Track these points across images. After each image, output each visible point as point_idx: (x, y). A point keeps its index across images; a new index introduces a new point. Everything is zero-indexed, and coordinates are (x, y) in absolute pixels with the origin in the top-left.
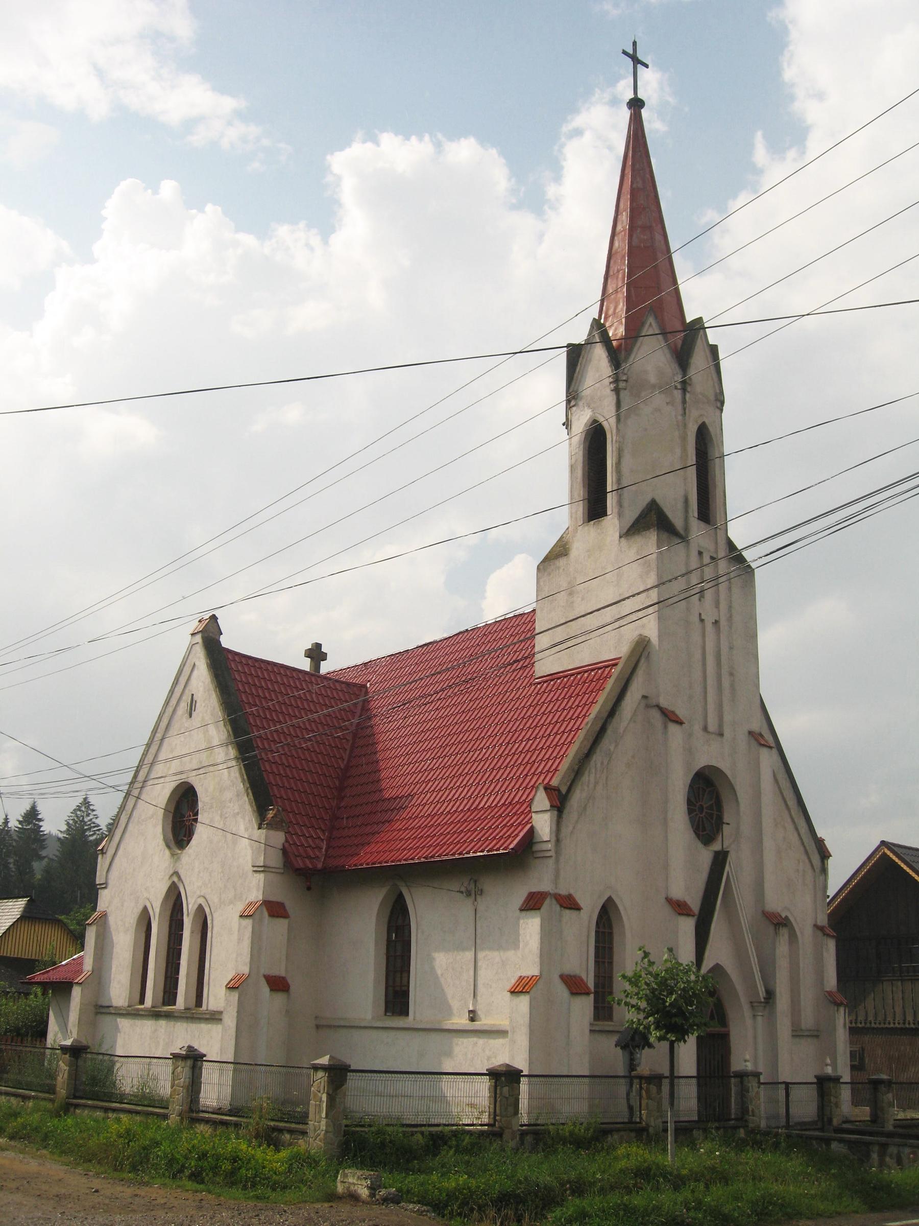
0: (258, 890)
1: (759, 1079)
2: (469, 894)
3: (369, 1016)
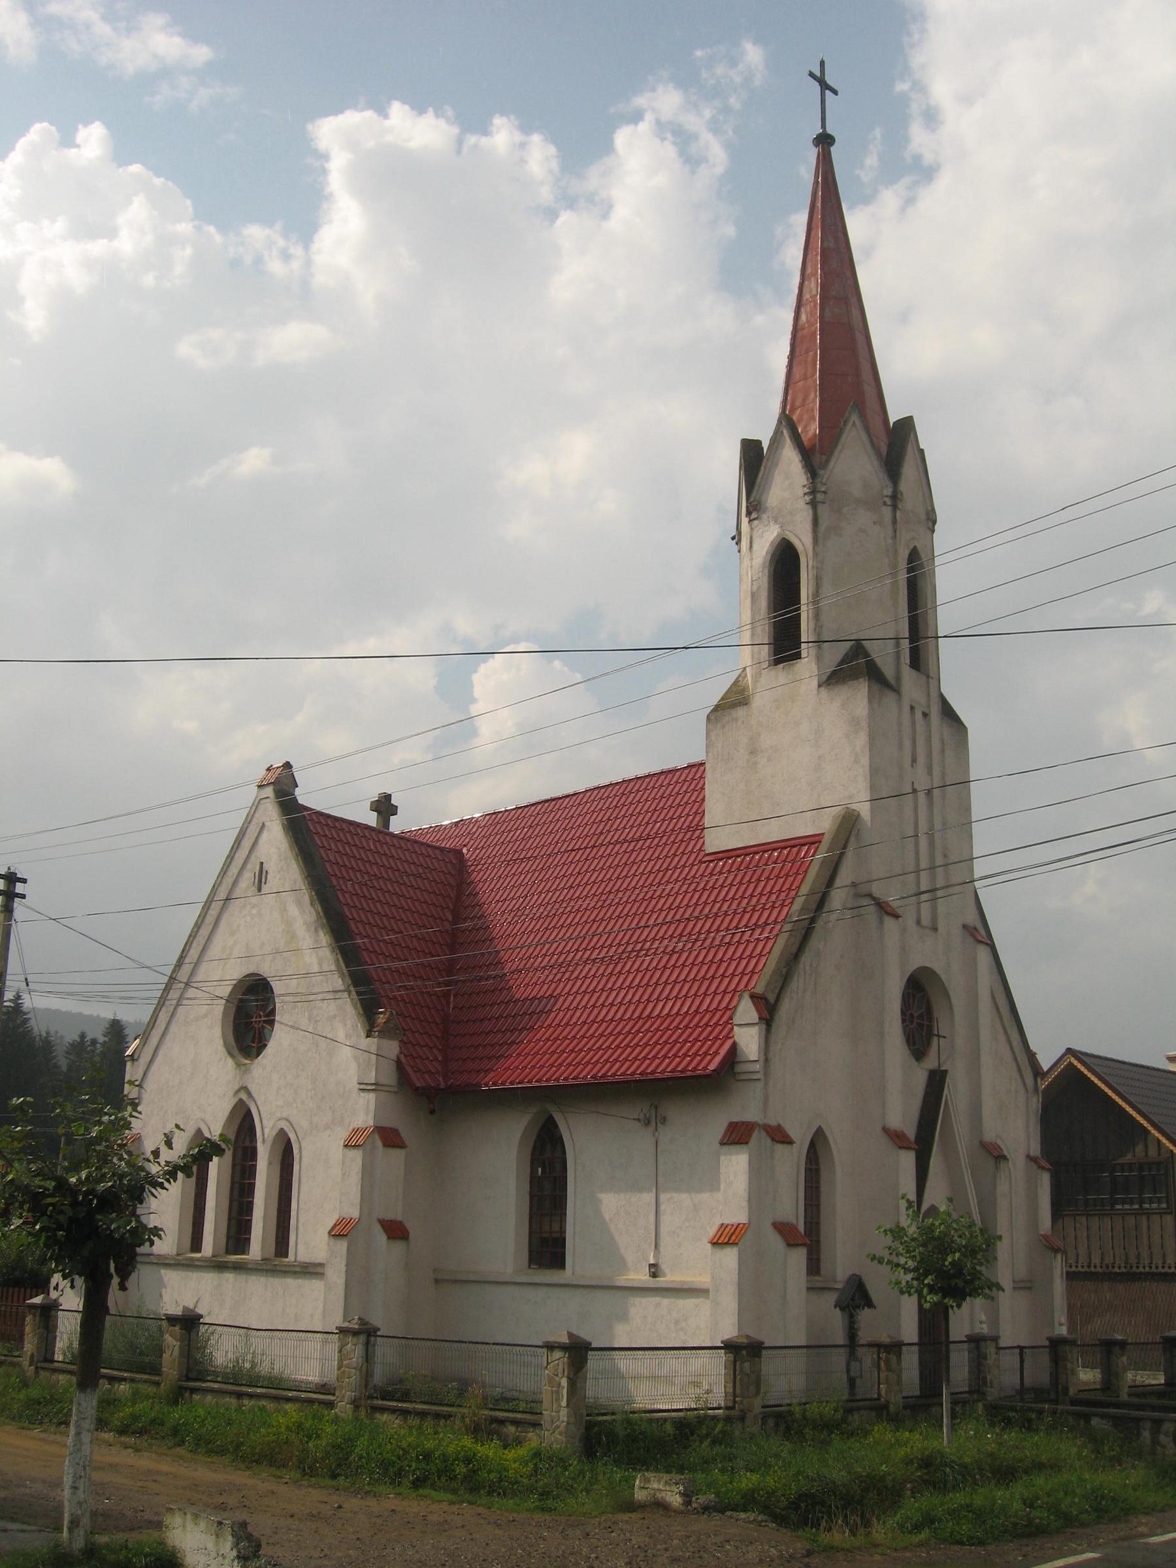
0: (367, 1114)
1: (997, 1343)
2: (647, 1123)
3: (510, 1270)
